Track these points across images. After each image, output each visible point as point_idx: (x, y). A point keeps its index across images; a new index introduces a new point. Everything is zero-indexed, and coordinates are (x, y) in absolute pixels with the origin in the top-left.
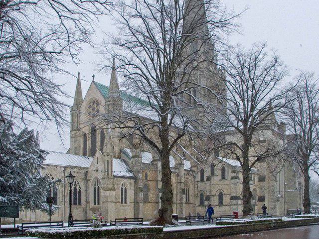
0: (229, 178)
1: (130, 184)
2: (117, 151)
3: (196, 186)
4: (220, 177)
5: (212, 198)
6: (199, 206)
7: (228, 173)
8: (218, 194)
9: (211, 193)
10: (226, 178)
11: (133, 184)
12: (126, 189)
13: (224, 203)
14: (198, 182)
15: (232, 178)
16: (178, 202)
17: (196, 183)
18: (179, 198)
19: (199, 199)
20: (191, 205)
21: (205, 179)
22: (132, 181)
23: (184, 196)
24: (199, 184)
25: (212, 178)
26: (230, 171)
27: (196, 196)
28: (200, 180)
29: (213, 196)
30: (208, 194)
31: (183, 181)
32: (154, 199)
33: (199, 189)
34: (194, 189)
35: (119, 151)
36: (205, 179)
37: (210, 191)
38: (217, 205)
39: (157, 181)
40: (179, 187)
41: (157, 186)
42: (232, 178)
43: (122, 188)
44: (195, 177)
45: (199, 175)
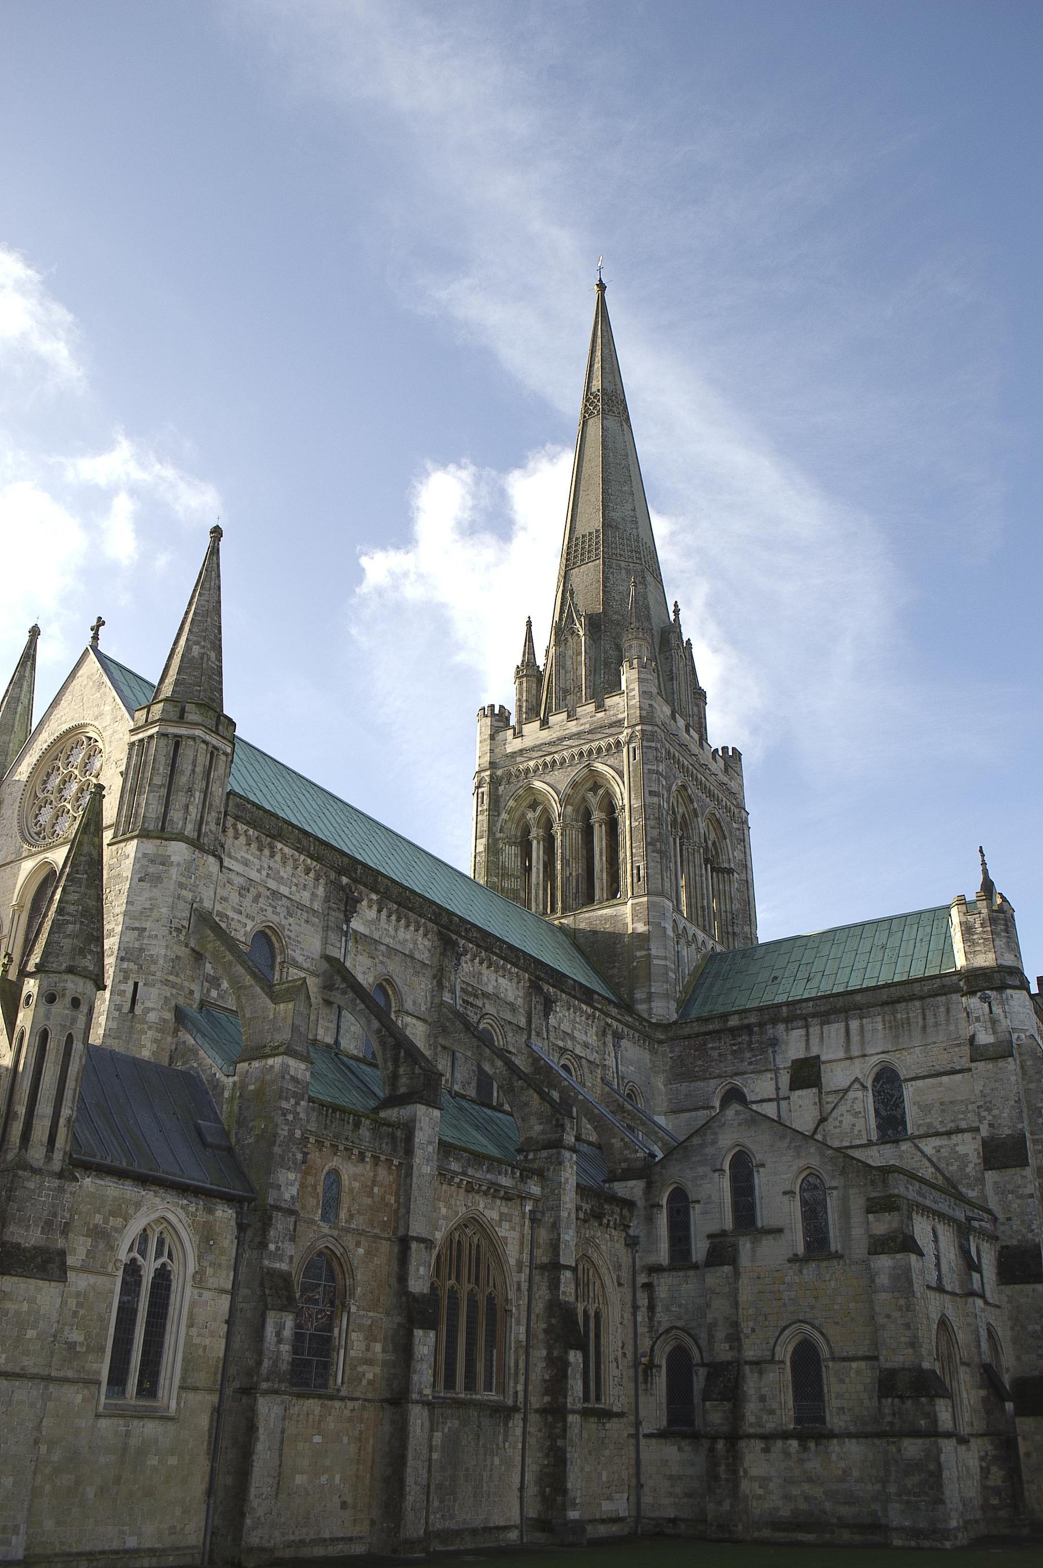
0: (859, 1248)
1: (207, 1238)
2: (152, 1017)
3: (643, 1301)
4: (797, 1239)
5: (751, 1385)
6: (662, 1435)
7: (845, 1214)
8: (785, 1352)
9: (740, 1350)
10: (835, 1244)
11: (228, 1241)
12: (163, 1277)
13: (835, 1421)
14: (654, 1269)
15: (879, 1246)
16: (536, 1402)
17: (642, 1279)
18: (539, 1371)
19: (661, 1381)
20: (613, 1425)
21: (699, 1249)
22: (224, 1215)
23: (575, 1357)
24: (664, 1284)
25: (745, 1246)
26: (857, 1204)
27: (644, 1370)
28: (663, 1254)
29: (757, 1364)
30: (723, 1352)
31: (567, 1258)
32: (370, 1373)
33: (663, 1319)
34: (628, 1315)
35: (169, 1016)
36: (699, 1249)
37: (735, 1339)
38: (786, 1436)
39: (404, 1243)
40: (542, 1293)
41: (402, 1278)
42: (879, 1246)
43: (132, 1270)
44: (632, 1243)
45: (663, 1220)
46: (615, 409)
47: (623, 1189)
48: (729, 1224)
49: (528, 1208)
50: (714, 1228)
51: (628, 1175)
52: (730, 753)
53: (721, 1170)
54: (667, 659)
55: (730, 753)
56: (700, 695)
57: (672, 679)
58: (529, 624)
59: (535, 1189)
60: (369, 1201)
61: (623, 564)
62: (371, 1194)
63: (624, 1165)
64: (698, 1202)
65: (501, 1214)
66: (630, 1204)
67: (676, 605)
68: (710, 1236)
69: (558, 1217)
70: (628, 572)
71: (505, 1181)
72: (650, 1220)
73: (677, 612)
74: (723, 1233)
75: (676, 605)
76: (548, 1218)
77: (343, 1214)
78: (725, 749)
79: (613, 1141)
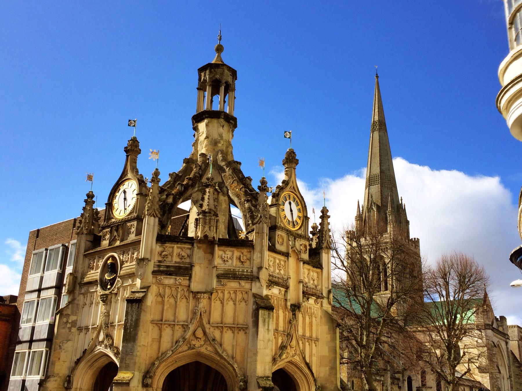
46: (382, 127)
47: (397, 376)
48: (421, 385)
49: (381, 383)
50: (417, 386)
51: (398, 372)
52: (416, 240)
53: (419, 374)
54: (399, 216)
55: (416, 240)
56: (407, 222)
57: (400, 223)
58: (358, 201)
59: (383, 379)
60: (358, 385)
61: (386, 185)
62: (358, 384)
63: (397, 370)
64: (414, 380)
65: (377, 384)
66: (398, 379)
67: (401, 198)
68: (416, 387)
69: (387, 385)
70: (387, 188)
71: (378, 378)
72: (403, 383)
73: (401, 200)
74: (419, 387)
75: (401, 198)
76: (385, 385)
77: (355, 388)
78: (415, 239)
79: (394, 365)
